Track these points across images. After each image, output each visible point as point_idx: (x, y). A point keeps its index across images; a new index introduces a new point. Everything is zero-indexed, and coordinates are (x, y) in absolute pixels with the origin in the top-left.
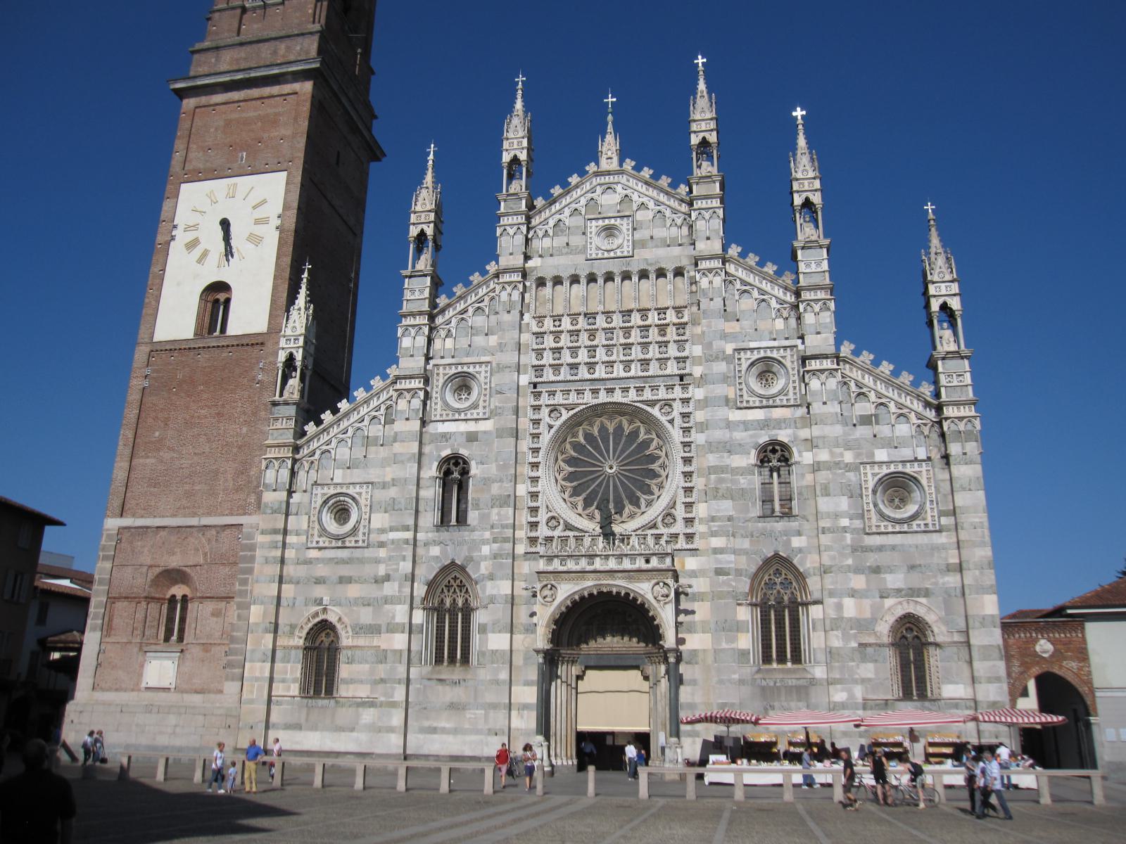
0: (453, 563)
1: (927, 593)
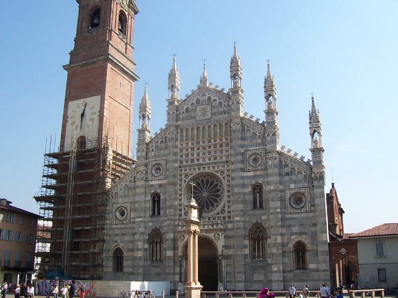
0: (156, 228)
1: (305, 234)
